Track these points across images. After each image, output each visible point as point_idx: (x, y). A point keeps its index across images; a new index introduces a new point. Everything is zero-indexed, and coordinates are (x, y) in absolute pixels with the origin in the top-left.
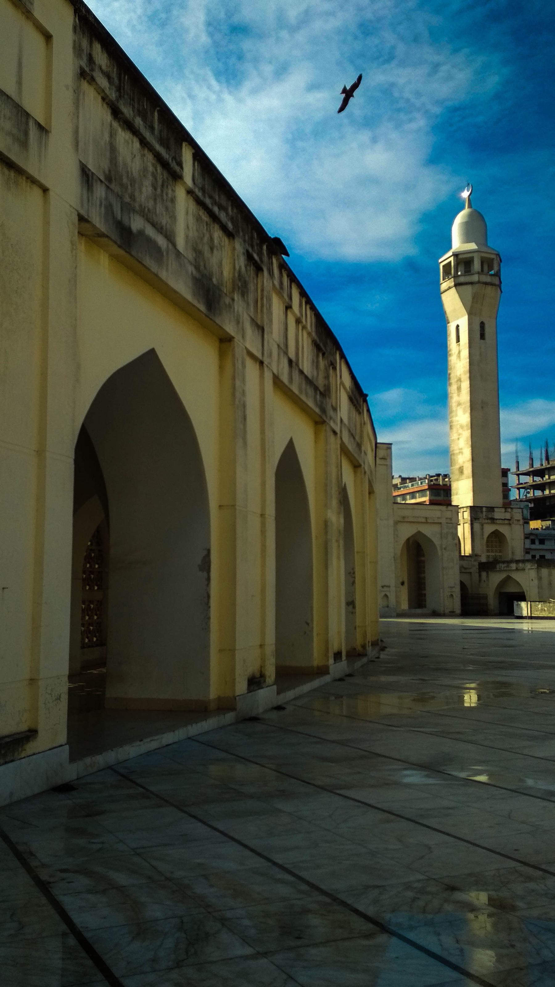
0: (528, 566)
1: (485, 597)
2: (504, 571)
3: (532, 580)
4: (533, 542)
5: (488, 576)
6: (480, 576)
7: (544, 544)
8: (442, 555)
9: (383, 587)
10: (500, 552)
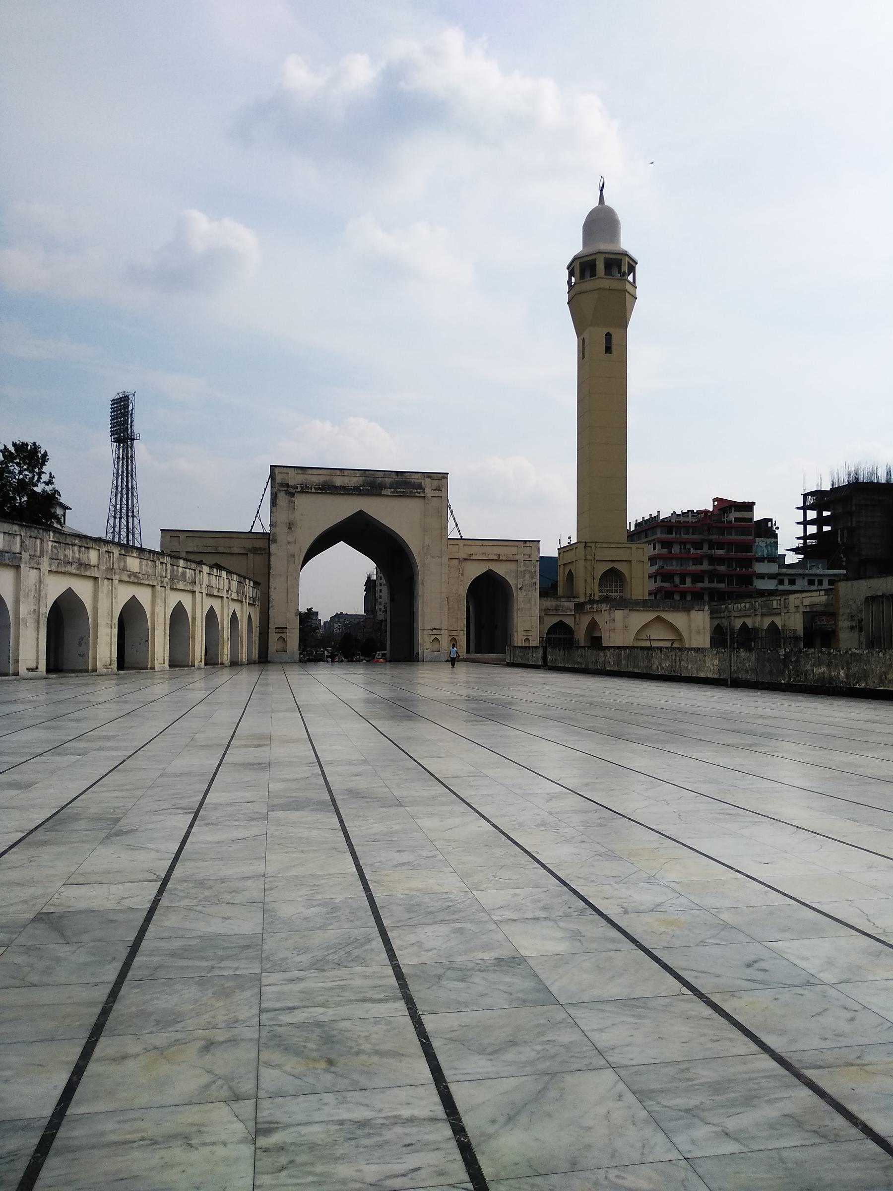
0: (604, 607)
4: (781, 582)
7: (794, 584)
10: (622, 591)
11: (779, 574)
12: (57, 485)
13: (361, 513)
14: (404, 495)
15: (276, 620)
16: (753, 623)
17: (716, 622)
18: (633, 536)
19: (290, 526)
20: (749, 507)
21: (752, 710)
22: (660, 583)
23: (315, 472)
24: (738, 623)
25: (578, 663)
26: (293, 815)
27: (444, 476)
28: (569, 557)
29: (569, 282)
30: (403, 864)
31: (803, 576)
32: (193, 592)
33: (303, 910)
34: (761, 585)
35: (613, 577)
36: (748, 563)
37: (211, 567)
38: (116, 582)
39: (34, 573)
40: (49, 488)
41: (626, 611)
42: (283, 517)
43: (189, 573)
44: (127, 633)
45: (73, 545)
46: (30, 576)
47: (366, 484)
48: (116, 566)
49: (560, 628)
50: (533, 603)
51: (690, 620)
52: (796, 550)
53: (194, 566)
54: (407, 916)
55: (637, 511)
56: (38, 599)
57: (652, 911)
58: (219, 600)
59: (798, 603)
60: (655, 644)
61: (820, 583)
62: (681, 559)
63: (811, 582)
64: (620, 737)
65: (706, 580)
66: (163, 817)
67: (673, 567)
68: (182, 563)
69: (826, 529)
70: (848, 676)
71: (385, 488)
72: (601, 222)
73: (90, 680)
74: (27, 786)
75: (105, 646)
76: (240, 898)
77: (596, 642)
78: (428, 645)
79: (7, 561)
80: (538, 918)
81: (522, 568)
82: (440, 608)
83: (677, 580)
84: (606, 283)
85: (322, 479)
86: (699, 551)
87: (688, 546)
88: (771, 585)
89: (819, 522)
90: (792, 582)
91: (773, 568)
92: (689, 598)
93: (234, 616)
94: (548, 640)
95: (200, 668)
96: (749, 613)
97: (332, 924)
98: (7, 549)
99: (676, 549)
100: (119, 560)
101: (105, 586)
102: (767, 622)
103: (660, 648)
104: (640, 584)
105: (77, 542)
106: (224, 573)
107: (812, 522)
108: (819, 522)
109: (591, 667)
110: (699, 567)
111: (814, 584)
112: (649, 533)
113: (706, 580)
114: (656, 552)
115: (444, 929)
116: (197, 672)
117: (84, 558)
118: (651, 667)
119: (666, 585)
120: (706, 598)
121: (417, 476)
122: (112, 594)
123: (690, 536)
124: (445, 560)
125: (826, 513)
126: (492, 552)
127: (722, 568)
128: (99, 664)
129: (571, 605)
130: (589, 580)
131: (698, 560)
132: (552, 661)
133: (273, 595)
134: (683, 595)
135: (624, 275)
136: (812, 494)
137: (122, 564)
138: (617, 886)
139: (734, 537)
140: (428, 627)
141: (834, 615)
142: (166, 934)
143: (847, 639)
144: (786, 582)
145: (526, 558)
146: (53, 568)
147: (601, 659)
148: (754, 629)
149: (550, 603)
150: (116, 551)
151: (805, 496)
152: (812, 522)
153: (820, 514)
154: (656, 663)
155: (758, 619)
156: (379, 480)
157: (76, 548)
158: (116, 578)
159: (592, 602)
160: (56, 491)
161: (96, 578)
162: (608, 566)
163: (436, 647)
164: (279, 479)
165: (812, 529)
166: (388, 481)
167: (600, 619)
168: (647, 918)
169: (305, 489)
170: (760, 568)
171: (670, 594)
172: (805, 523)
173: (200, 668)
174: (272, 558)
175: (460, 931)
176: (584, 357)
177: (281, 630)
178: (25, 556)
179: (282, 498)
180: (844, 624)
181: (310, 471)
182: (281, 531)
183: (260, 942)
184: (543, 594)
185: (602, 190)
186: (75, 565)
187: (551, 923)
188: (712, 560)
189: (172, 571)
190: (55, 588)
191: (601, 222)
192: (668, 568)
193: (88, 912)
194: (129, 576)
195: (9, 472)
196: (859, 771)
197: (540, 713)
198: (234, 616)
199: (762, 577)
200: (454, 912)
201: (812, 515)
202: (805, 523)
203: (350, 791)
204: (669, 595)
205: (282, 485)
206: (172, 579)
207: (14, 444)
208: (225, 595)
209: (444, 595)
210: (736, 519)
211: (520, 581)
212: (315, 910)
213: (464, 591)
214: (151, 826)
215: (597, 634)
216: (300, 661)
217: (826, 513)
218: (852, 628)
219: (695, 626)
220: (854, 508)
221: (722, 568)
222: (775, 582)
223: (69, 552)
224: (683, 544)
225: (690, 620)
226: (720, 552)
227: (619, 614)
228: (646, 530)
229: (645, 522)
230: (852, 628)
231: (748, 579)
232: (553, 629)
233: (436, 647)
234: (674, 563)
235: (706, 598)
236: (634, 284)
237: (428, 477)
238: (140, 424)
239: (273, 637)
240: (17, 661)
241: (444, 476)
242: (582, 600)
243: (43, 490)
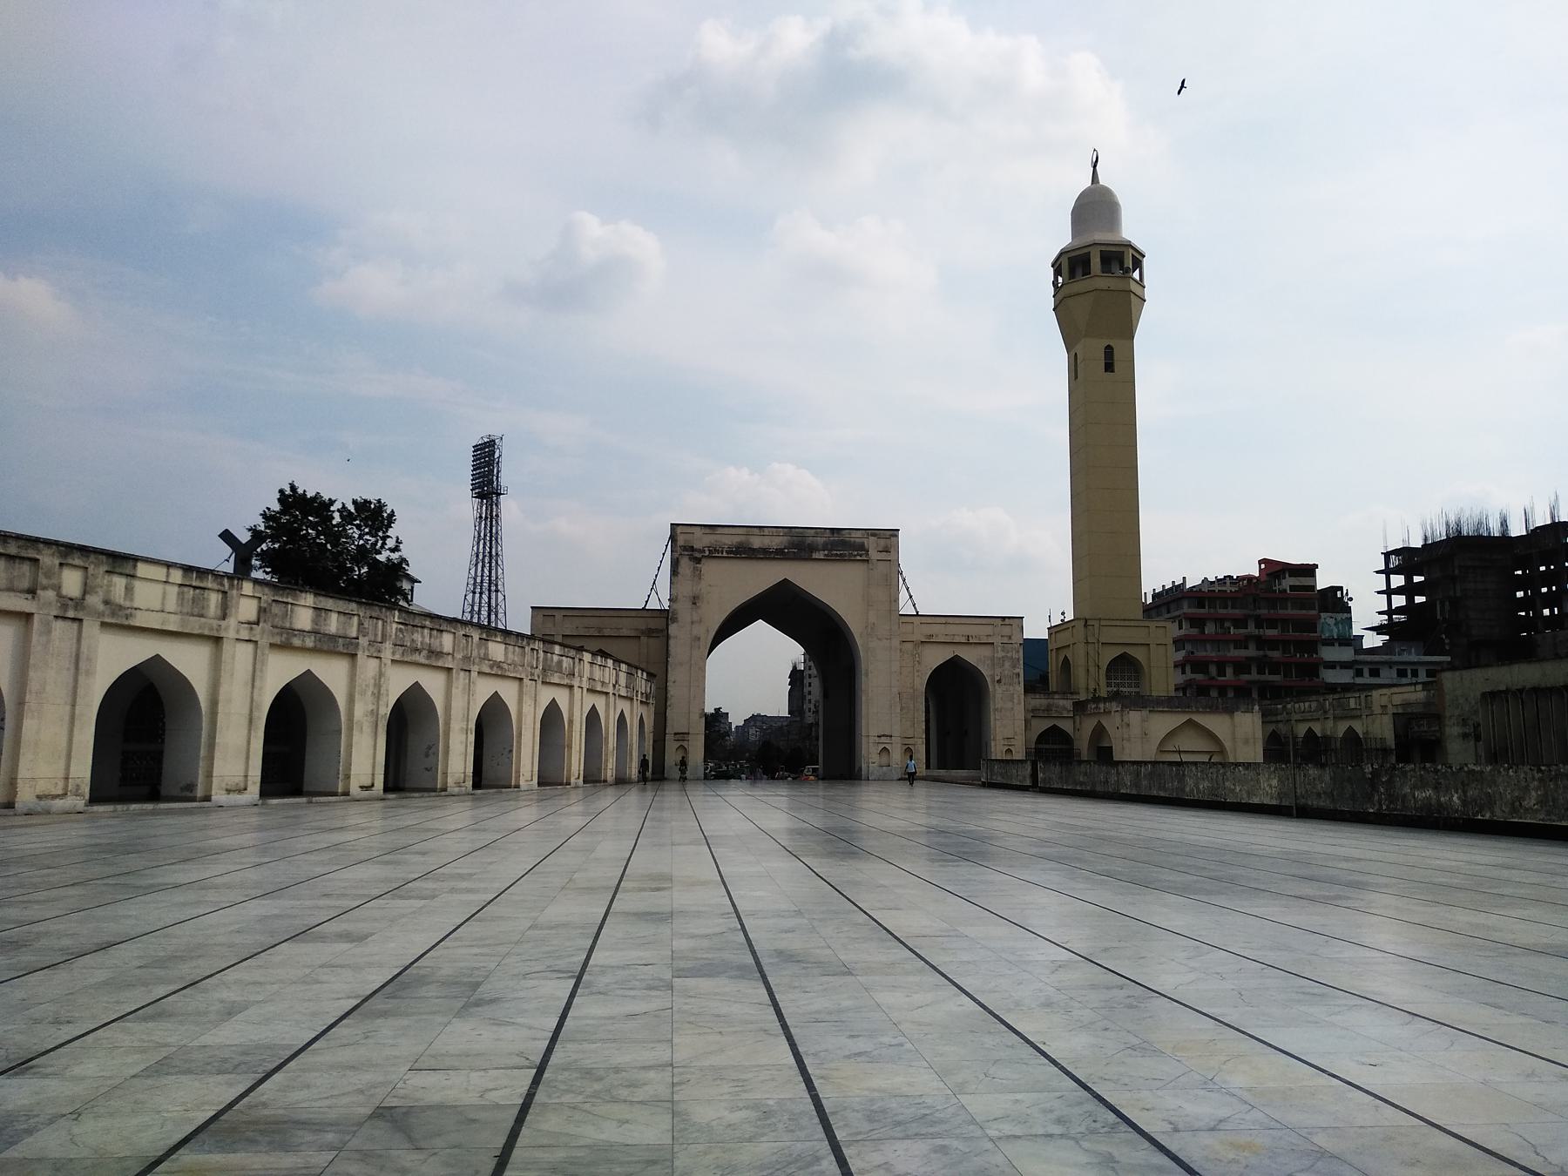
0: (1114, 706)
4: (1359, 673)
11: (1355, 662)
12: (405, 552)
13: (785, 584)
14: (842, 559)
15: (676, 722)
16: (1323, 730)
17: (1271, 727)
18: (1149, 611)
19: (695, 600)
20: (1309, 570)
21: (1330, 850)
22: (1189, 675)
23: (726, 531)
24: (1301, 730)
25: (1082, 784)
26: (705, 984)
27: (894, 533)
28: (1063, 639)
29: (1055, 283)
30: (859, 1054)
31: (1390, 664)
32: (571, 687)
33: (726, 1113)
34: (1331, 676)
35: (1124, 666)
36: (1312, 646)
37: (594, 654)
38: (474, 674)
39: (374, 663)
40: (395, 556)
41: (1145, 713)
42: (686, 589)
43: (566, 662)
44: (486, 740)
45: (423, 627)
46: (368, 667)
47: (792, 545)
48: (475, 653)
49: (1054, 734)
52: (1378, 630)
53: (572, 653)
54: (866, 1126)
55: (1155, 577)
56: (377, 696)
57: (1212, 1129)
58: (603, 698)
59: (1384, 701)
60: (1185, 758)
61: (1415, 674)
62: (1216, 641)
63: (1402, 673)
64: (1146, 884)
65: (1254, 670)
66: (535, 982)
67: (1209, 652)
68: (557, 649)
69: (1419, 599)
70: (1464, 803)
72: (1095, 206)
73: (438, 802)
74: (361, 938)
75: (458, 759)
76: (640, 1094)
77: (1104, 755)
78: (874, 757)
79: (341, 649)
80: (1051, 1136)
81: (1001, 654)
82: (889, 709)
83: (1213, 670)
84: (1103, 282)
85: (736, 540)
86: (1242, 631)
87: (1227, 624)
88: (1345, 677)
89: (1408, 590)
90: (1375, 673)
91: (1347, 654)
92: (1231, 694)
93: (622, 718)
94: (1038, 751)
95: (577, 787)
96: (1316, 715)
97: (763, 1135)
98: (341, 633)
99: (1210, 629)
100: (479, 647)
101: (460, 679)
102: (1342, 728)
103: (1195, 763)
104: (1163, 676)
105: (428, 623)
106: (610, 662)
107: (1399, 591)
108: (1408, 590)
109: (1099, 788)
110: (1242, 653)
111: (1405, 675)
112: (1172, 606)
113: (1254, 670)
114: (1182, 632)
115: (920, 1147)
116: (573, 792)
117: (435, 644)
118: (1183, 790)
119: (1199, 677)
120: (1255, 695)
121: (859, 534)
122: (469, 690)
123: (1230, 611)
124: (896, 643)
125: (1417, 579)
126: (959, 632)
127: (1275, 655)
128: (450, 781)
129: (1068, 704)
131: (1241, 643)
132: (1044, 780)
133: (673, 690)
134: (1222, 690)
135: (1127, 271)
136: (1396, 552)
137: (482, 652)
138: (1159, 1093)
139: (1290, 612)
140: (874, 732)
141: (1437, 718)
142: (545, 1142)
143: (1458, 751)
144: (1366, 672)
146: (397, 657)
147: (1113, 779)
148: (1327, 739)
149: (1039, 701)
150: (476, 635)
151: (1387, 555)
152: (1399, 591)
153: (1409, 579)
154: (1190, 782)
155: (1330, 724)
157: (426, 631)
158: (475, 668)
159: (1097, 699)
160: (403, 560)
161: (449, 670)
162: (1117, 652)
163: (884, 760)
164: (681, 541)
165: (1399, 601)
166: (820, 540)
167: (1111, 724)
168: (1206, 1139)
169: (714, 553)
170: (1329, 654)
171: (1204, 689)
172: (1389, 592)
173: (577, 787)
174: (671, 642)
175: (943, 1150)
177: (682, 736)
178: (363, 641)
179: (685, 565)
180: (1453, 730)
181: (720, 530)
182: (683, 609)
183: (669, 1156)
184: (1030, 689)
186: (424, 653)
187: (1072, 1143)
188: (1261, 643)
189: (545, 659)
190: (398, 682)
191: (1095, 206)
192: (1200, 654)
193: (440, 1107)
194: (491, 667)
195: (347, 537)
196: (1496, 936)
197: (1034, 850)
198: (622, 718)
199: (1332, 665)
200: (933, 1123)
201: (1398, 581)
202: (1389, 592)
203: (780, 953)
204: (1202, 690)
205: (685, 548)
206: (544, 670)
207: (355, 502)
208: (610, 690)
209: (895, 690)
210: (1293, 588)
211: (998, 671)
212: (743, 1114)
213: (921, 683)
214: (521, 994)
215: (1106, 745)
216: (706, 777)
217: (1417, 579)
218: (1465, 736)
219: (1241, 733)
221: (1275, 655)
222: (1351, 672)
223: (417, 637)
224: (1220, 621)
225: (1234, 726)
226: (1271, 633)
227: (1134, 717)
228: (1167, 604)
229: (1166, 592)
230: (1465, 736)
231: (1312, 669)
232: (1043, 737)
233: (884, 760)
234: (1208, 647)
235: (1255, 695)
236: (1141, 283)
238: (508, 474)
239: (671, 746)
240: (348, 777)
241: (894, 533)
242: (1083, 697)
243: (388, 559)
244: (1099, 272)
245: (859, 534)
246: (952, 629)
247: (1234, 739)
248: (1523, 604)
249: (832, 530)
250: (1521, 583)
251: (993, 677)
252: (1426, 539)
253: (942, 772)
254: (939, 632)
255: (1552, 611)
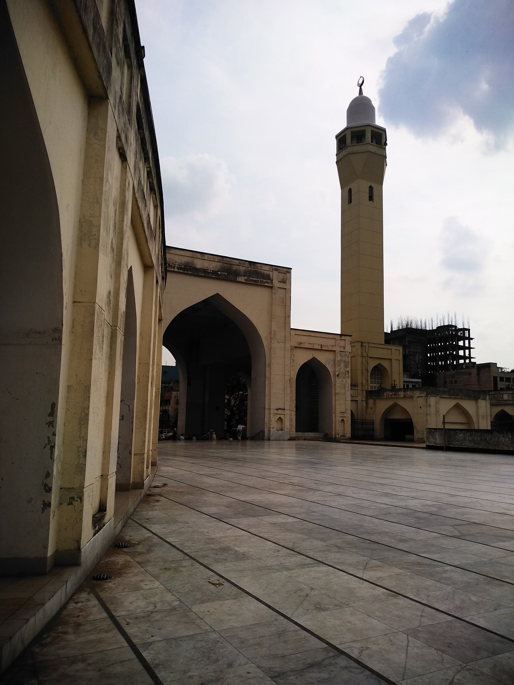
0: (417, 393)
1: (372, 423)
2: (391, 398)
3: (421, 407)
5: (374, 404)
6: (367, 403)
8: (335, 381)
9: (277, 410)
14: (255, 284)
17: (497, 410)
35: (379, 371)
41: (438, 398)
47: (223, 269)
50: (347, 388)
51: (477, 407)
71: (240, 275)
81: (339, 358)
85: (184, 260)
126: (317, 342)
130: (364, 372)
145: (342, 349)
156: (235, 268)
166: (242, 269)
176: (350, 201)
185: (361, 86)
211: (337, 369)
213: (294, 375)
220: (407, 343)
237: (276, 270)
244: (370, 142)
245: (267, 268)
246: (312, 340)
247: (478, 415)
248: (431, 359)
249: (250, 262)
250: (430, 350)
251: (335, 372)
252: (407, 325)
253: (300, 434)
254: (306, 341)
255: (442, 363)
